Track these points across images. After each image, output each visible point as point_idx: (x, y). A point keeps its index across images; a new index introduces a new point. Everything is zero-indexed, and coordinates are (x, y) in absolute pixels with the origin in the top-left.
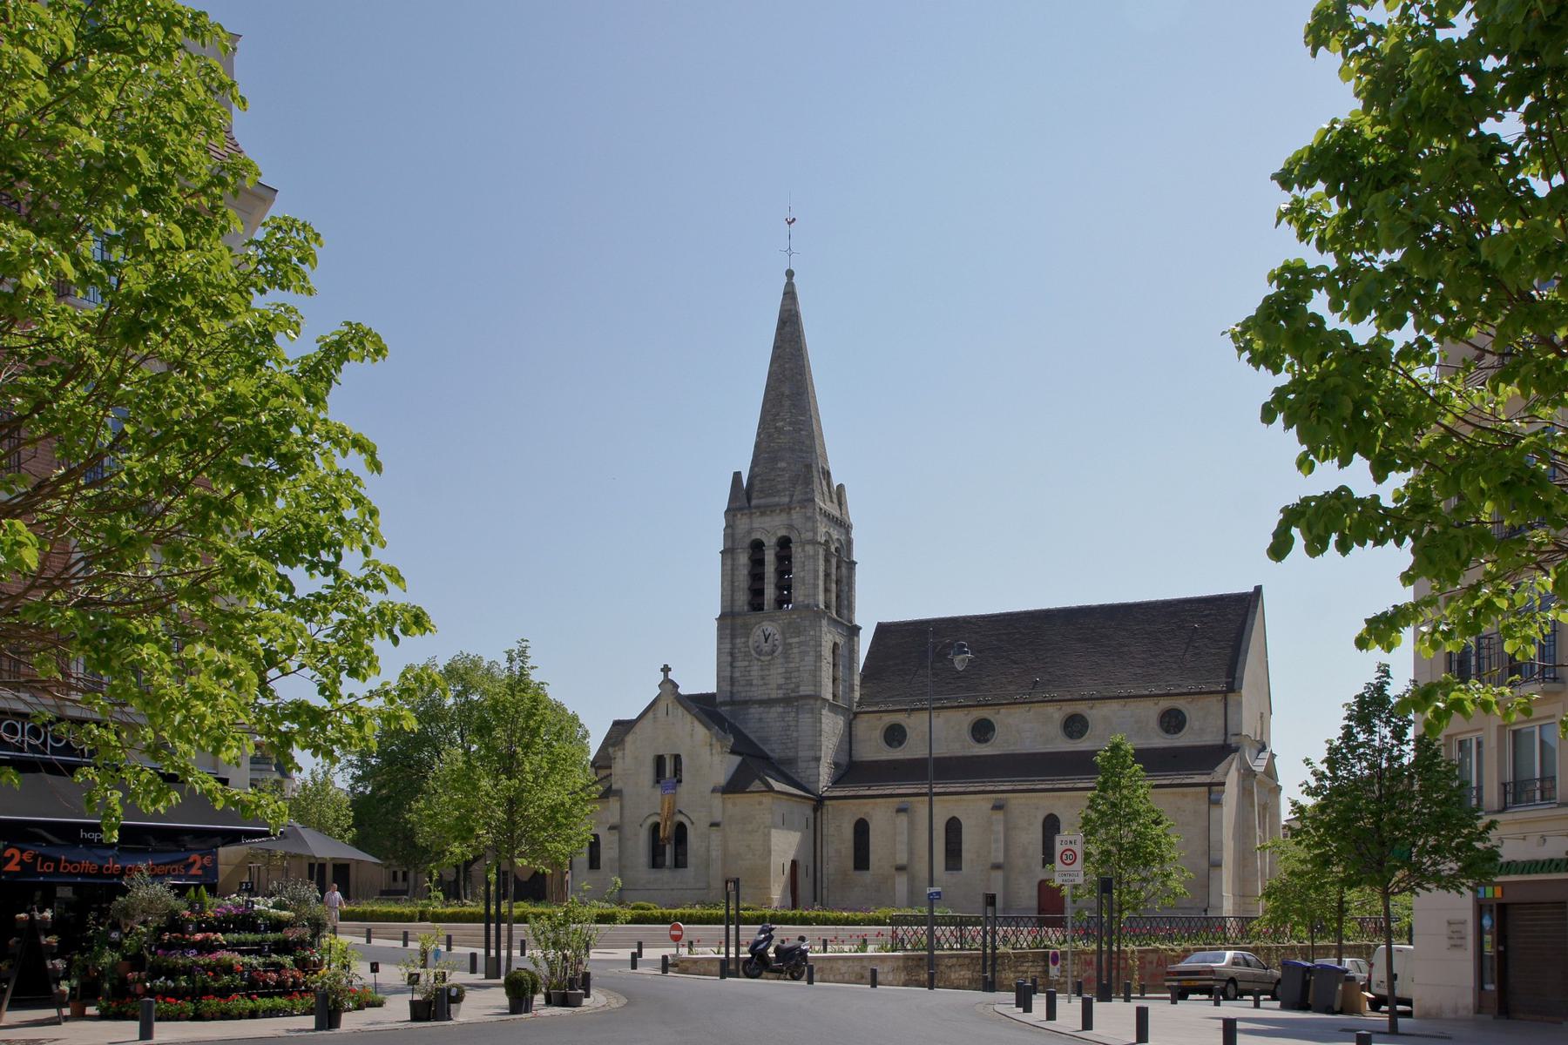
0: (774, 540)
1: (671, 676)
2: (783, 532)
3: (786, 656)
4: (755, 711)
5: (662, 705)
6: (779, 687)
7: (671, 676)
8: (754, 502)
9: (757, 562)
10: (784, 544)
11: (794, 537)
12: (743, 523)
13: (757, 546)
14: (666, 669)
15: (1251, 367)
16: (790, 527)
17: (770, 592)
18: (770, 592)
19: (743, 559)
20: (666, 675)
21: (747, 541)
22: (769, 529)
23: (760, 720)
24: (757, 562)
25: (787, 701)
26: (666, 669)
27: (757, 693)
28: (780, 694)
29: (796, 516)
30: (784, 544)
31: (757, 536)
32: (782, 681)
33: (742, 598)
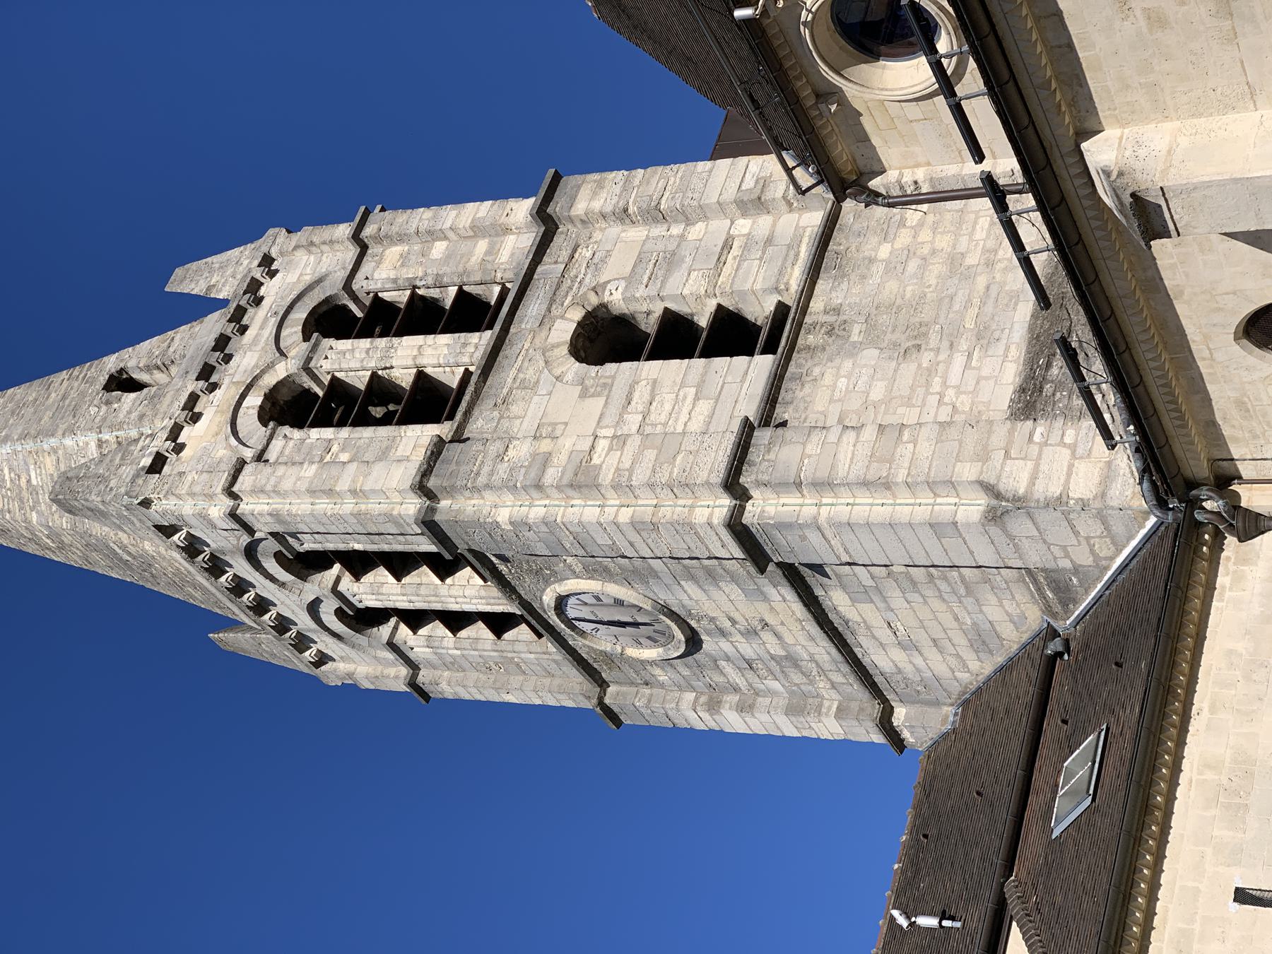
2: (272, 566)
23: (908, 646)
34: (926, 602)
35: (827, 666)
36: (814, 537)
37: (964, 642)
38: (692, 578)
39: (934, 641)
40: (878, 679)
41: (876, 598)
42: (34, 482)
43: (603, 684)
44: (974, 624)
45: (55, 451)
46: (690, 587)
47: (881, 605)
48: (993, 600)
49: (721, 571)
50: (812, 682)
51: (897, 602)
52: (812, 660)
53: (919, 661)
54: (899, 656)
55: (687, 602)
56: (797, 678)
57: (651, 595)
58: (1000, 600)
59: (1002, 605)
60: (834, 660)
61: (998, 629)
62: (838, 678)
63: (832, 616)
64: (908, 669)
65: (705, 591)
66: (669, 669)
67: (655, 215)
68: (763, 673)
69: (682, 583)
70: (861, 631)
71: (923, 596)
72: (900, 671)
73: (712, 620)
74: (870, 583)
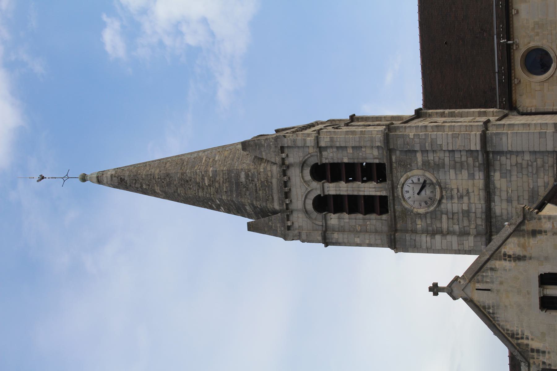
0: (315, 185)
1: (443, 283)
2: (307, 172)
3: (438, 167)
4: (499, 207)
5: (478, 297)
6: (472, 176)
7: (443, 283)
8: (277, 207)
9: (339, 204)
10: (320, 172)
11: (314, 161)
12: (299, 220)
13: (323, 204)
14: (435, 289)
15: (351, 114)
16: (303, 164)
17: (369, 189)
18: (369, 189)
19: (334, 219)
20: (442, 290)
21: (315, 214)
22: (304, 189)
23: (509, 200)
24: (339, 204)
25: (488, 167)
26: (435, 289)
27: (477, 204)
28: (480, 176)
29: (294, 158)
30: (320, 172)
31: (310, 203)
32: (465, 173)
33: (375, 221)
34: (522, 178)
35: (479, 215)
36: (504, 138)
37: (526, 197)
38: (455, 168)
39: (518, 197)
40: (493, 220)
41: (508, 175)
42: (217, 158)
43: (396, 231)
44: (533, 188)
45: (231, 149)
46: (452, 172)
47: (508, 179)
48: (542, 174)
49: (465, 163)
50: (469, 226)
51: (514, 178)
52: (475, 213)
53: (510, 209)
54: (504, 205)
55: (448, 181)
56: (466, 223)
57: (438, 177)
58: (544, 175)
59: (544, 178)
60: (482, 213)
61: (539, 190)
62: (479, 222)
63: (491, 186)
64: (505, 212)
65: (456, 174)
66: (424, 220)
67: (452, 115)
68: (455, 221)
69: (451, 170)
70: (498, 193)
71: (523, 174)
72: (501, 215)
73: (452, 190)
74: (509, 168)
